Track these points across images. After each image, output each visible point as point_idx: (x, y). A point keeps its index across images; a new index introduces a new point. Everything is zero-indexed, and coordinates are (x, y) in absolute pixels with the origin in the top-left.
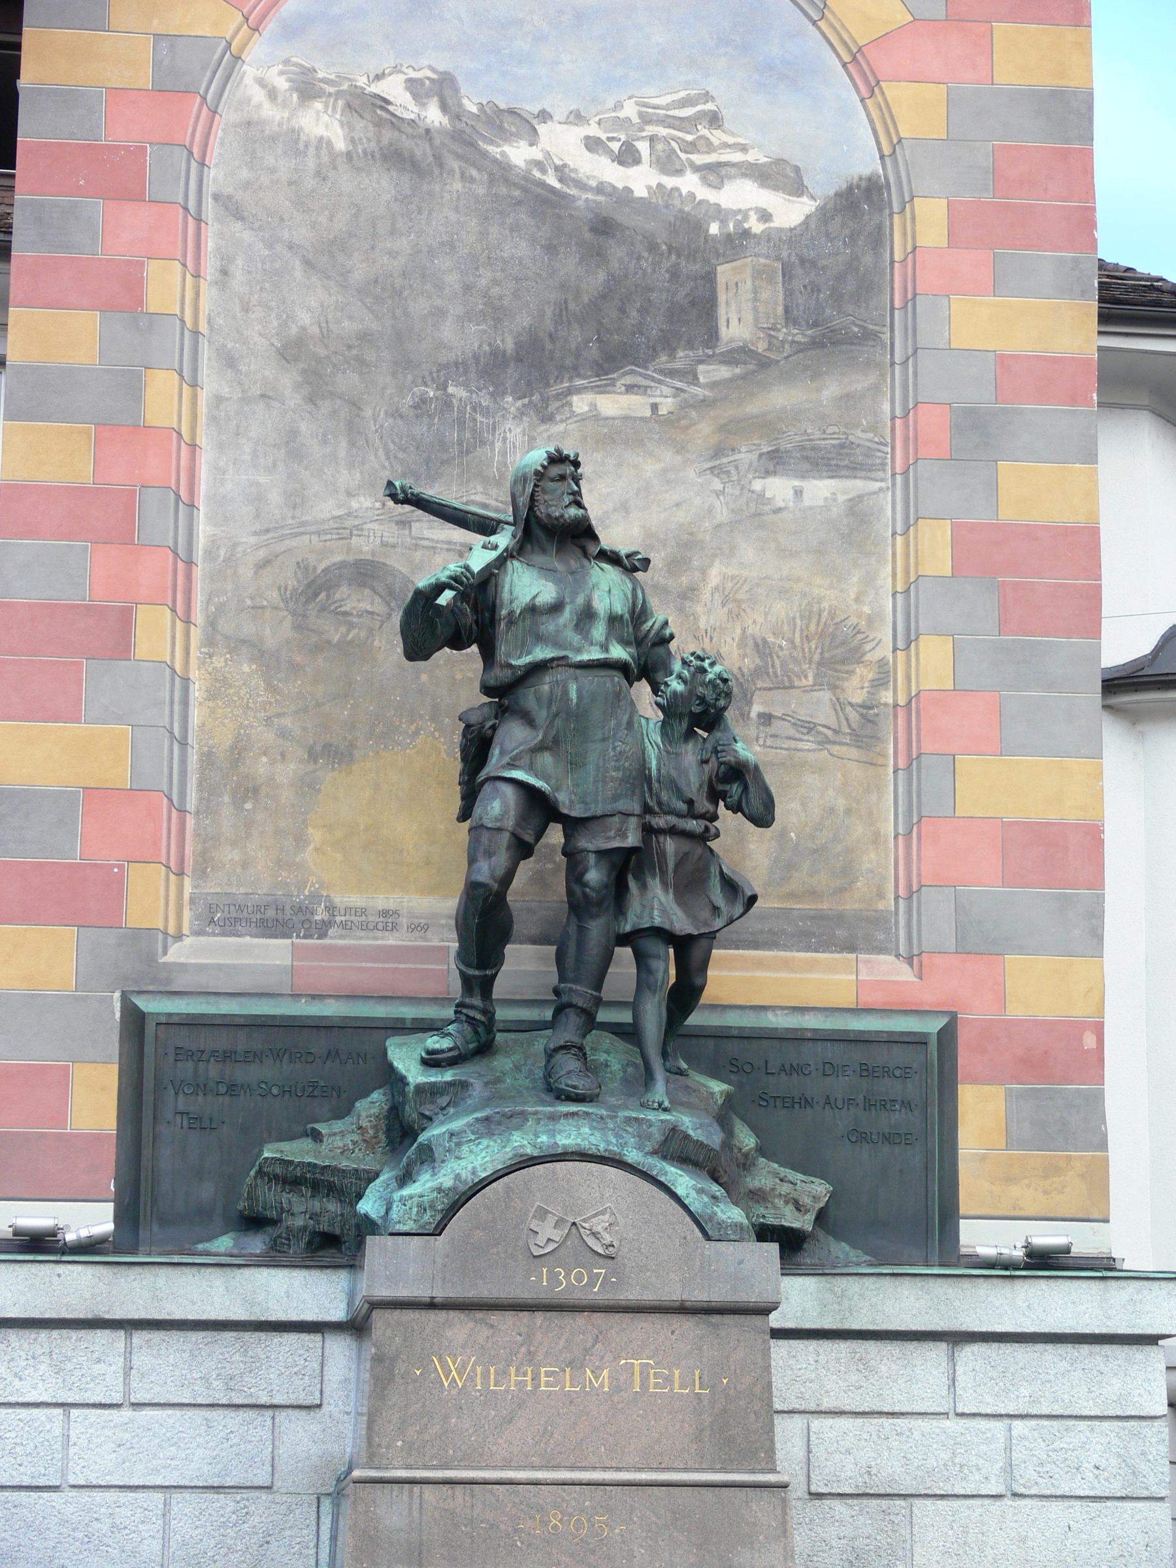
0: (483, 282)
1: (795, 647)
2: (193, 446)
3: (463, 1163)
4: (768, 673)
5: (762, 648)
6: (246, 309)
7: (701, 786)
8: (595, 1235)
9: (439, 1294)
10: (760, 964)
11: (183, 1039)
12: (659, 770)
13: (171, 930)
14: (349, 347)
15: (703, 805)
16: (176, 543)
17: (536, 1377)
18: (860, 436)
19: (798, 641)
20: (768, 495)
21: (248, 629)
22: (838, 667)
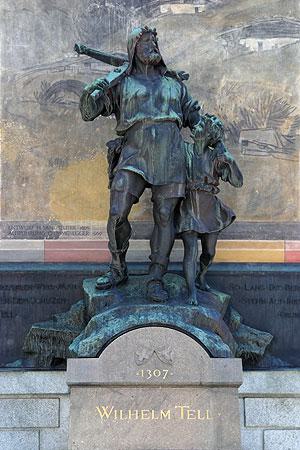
5: (244, 112)
8: (163, 356)
10: (243, 245)
18: (289, 18)
21: (22, 111)
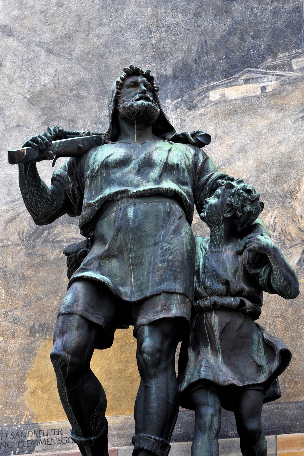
0: (154, 40)
6: (11, 82)
7: (236, 271)
12: (204, 265)
14: (71, 90)
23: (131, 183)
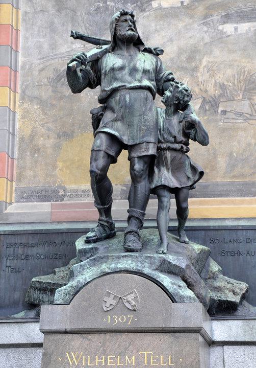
1: (235, 86)
2: (17, 30)
3: (82, 276)
4: (225, 96)
5: (222, 87)
7: (179, 131)
8: (128, 302)
9: (69, 327)
10: (223, 203)
11: (9, 240)
12: (163, 126)
13: (8, 201)
15: (181, 138)
16: (11, 65)
17: (106, 360)
19: (236, 83)
20: (225, 31)
21: (36, 93)
22: (251, 91)
23: (127, 81)
